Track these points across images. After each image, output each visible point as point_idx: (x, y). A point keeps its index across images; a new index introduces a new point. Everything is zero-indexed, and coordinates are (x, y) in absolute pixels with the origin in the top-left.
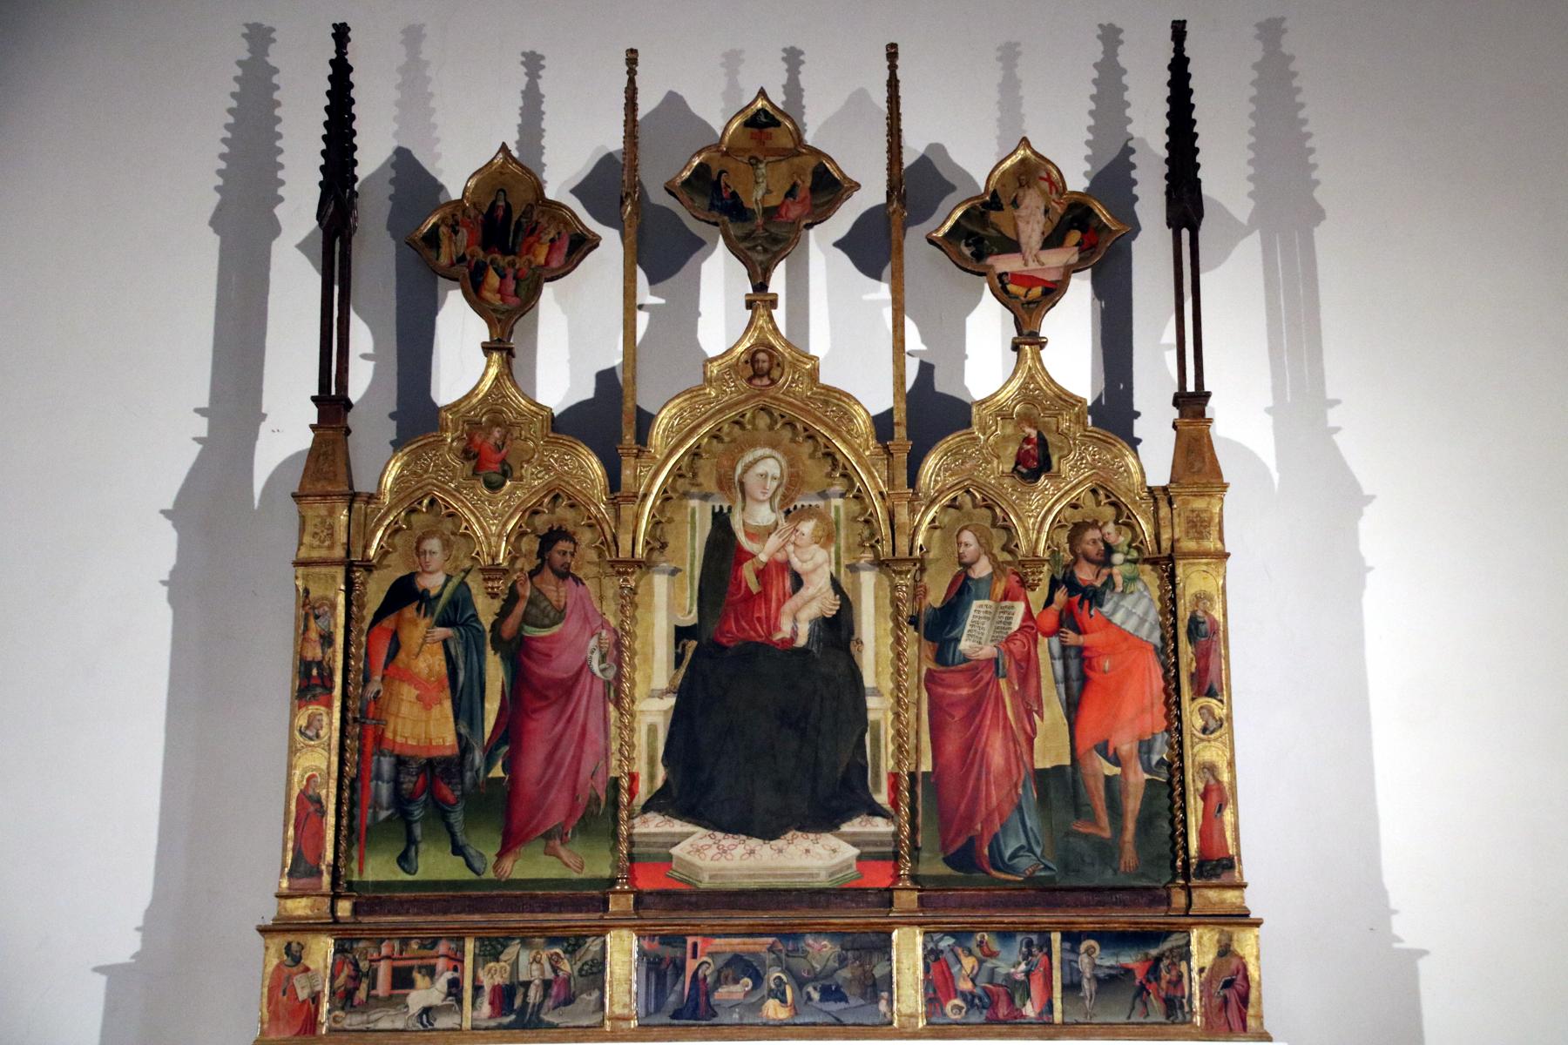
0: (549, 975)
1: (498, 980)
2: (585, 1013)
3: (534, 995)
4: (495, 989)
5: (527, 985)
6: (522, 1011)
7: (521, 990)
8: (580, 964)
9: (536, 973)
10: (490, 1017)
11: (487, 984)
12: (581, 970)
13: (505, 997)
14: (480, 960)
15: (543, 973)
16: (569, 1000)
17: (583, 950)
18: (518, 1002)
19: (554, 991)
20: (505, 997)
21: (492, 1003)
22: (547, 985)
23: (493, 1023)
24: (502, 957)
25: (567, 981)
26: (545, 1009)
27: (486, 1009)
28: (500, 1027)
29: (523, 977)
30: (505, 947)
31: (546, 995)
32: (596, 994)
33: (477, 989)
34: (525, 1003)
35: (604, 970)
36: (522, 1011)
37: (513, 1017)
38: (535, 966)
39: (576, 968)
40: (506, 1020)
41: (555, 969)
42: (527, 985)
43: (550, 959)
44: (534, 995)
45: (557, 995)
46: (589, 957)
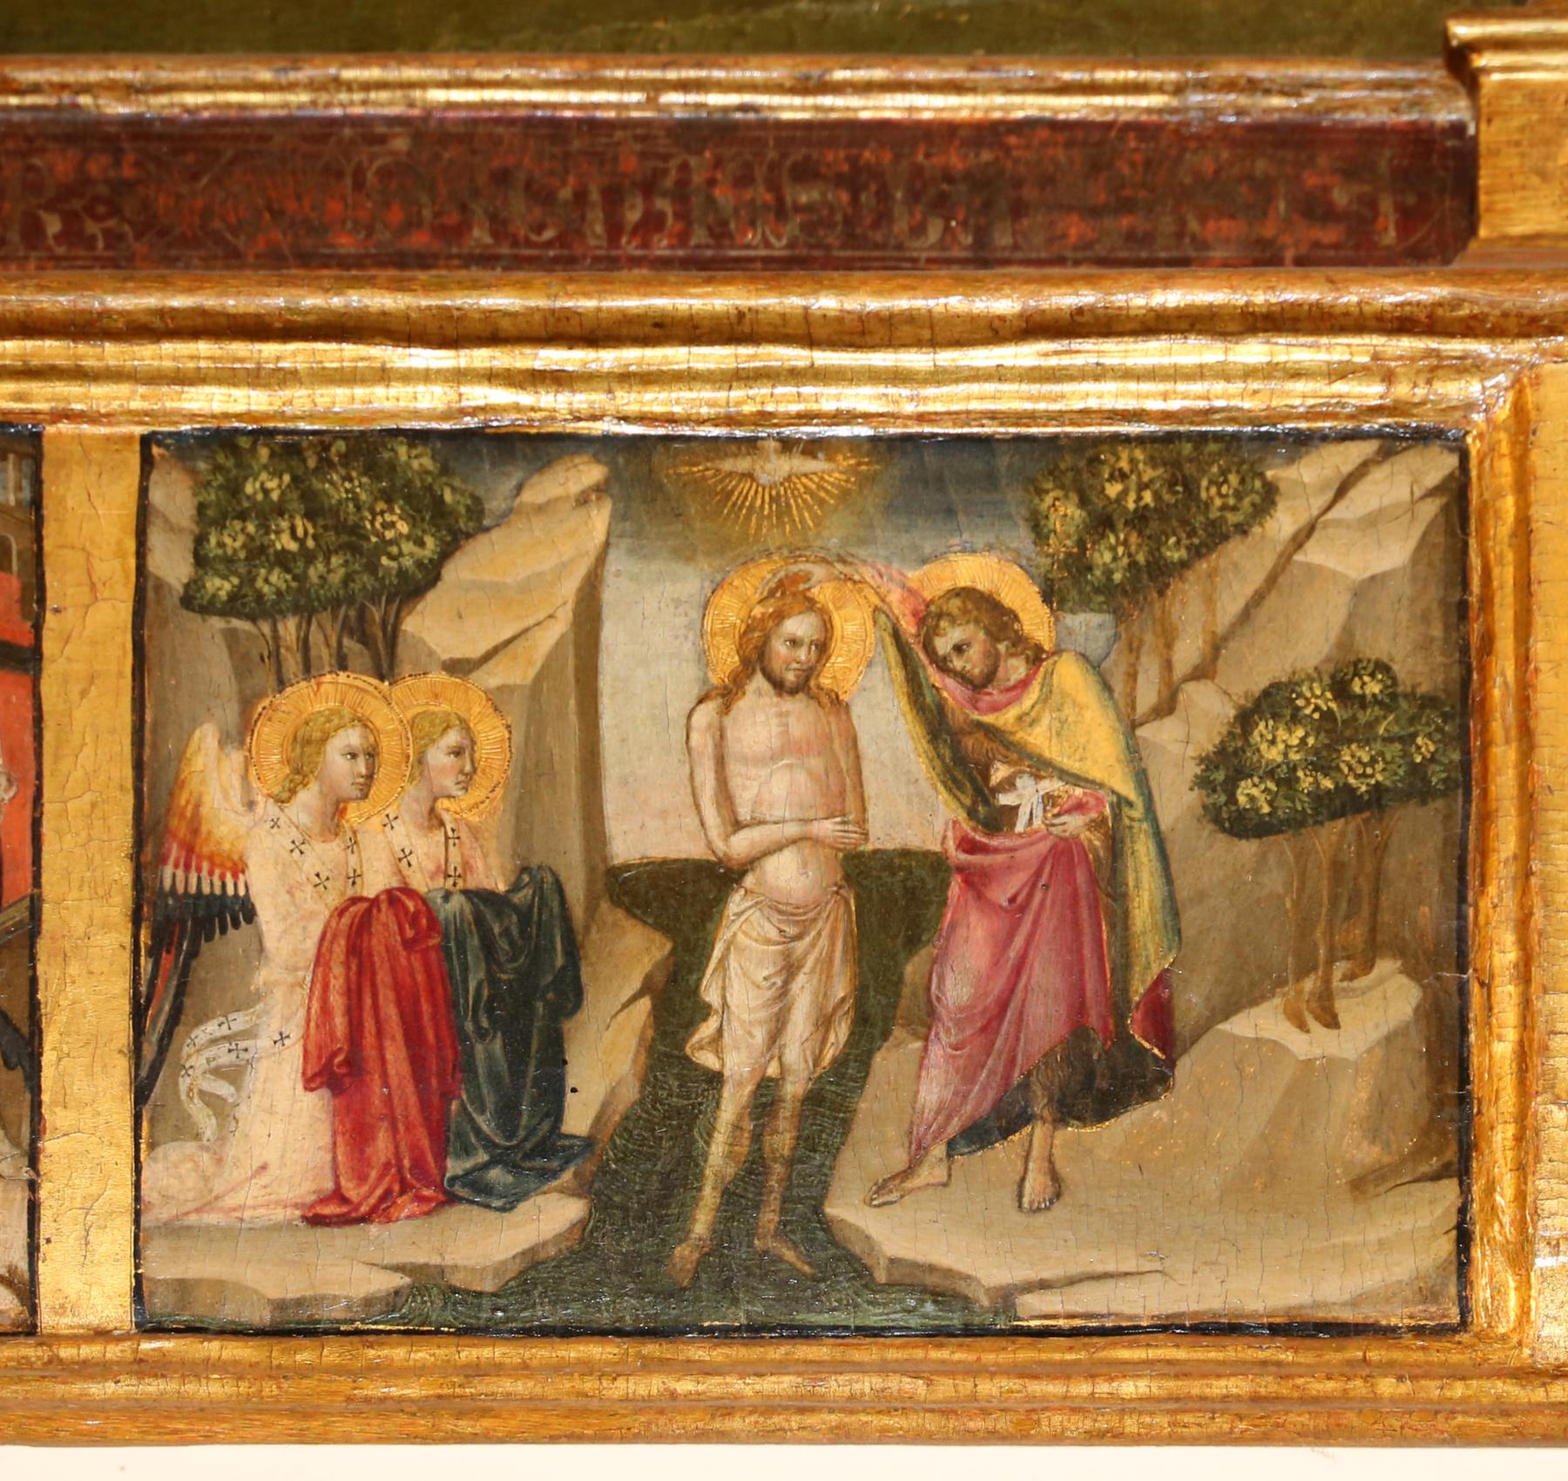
0: (911, 809)
1: (396, 848)
2: (1267, 1186)
3: (763, 1004)
4: (365, 933)
5: (685, 899)
6: (644, 1165)
7: (626, 957)
8: (1209, 710)
9: (776, 790)
10: (329, 1214)
11: (288, 875)
12: (1226, 764)
13: (466, 1016)
14: (206, 649)
15: (845, 787)
16: (1114, 1063)
17: (1242, 566)
18: (602, 1068)
19: (963, 966)
20: (466, 1016)
21: (336, 1072)
22: (890, 904)
23: (352, 1271)
24: (431, 627)
25: (1088, 878)
26: (872, 1147)
27: (277, 1131)
28: (434, 1309)
29: (645, 832)
30: (455, 529)
31: (879, 1006)
32: (1384, 1003)
33: (185, 929)
34: (676, 1076)
35: (1465, 780)
36: (644, 1165)
37: (552, 1215)
38: (760, 720)
39: (1179, 745)
40: (485, 1244)
41: (967, 759)
42: (685, 899)
43: (913, 653)
44: (763, 1004)
45: (996, 1014)
46: (1303, 643)
